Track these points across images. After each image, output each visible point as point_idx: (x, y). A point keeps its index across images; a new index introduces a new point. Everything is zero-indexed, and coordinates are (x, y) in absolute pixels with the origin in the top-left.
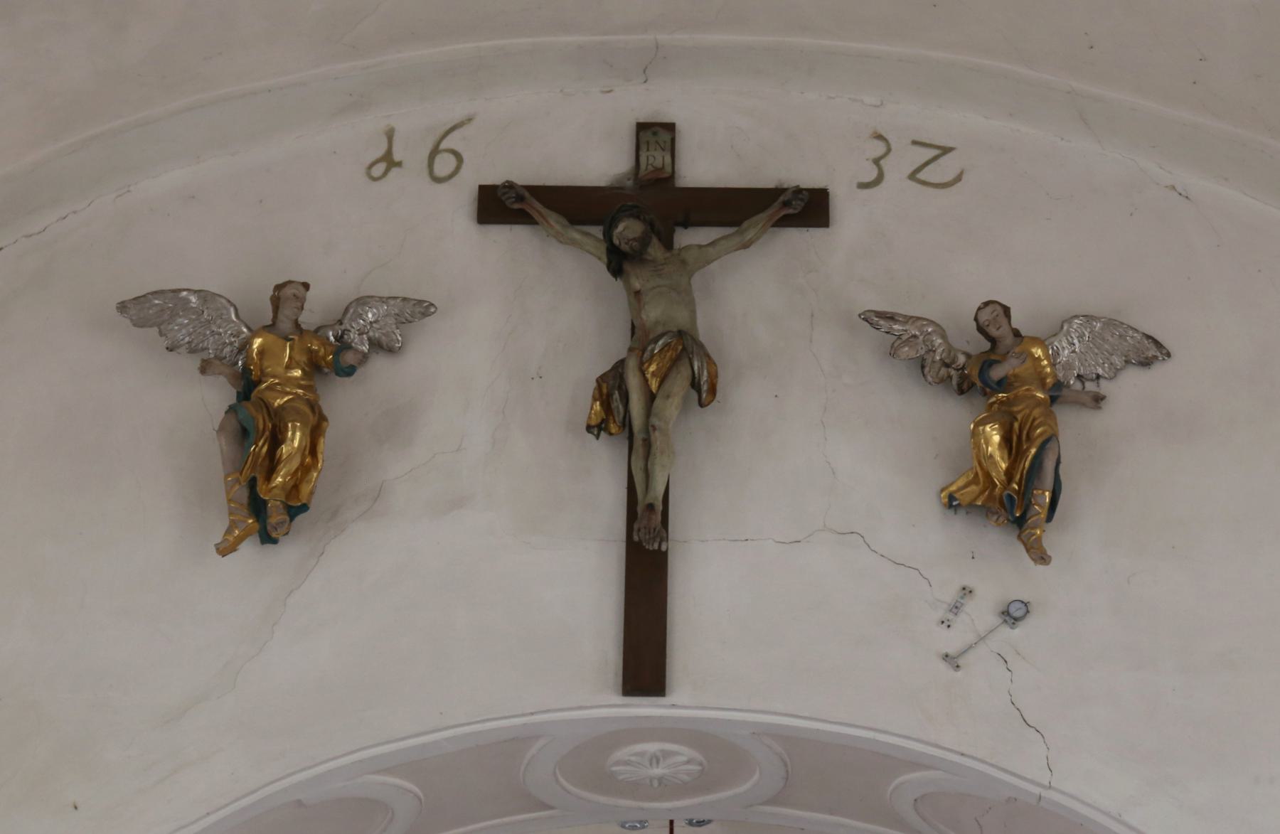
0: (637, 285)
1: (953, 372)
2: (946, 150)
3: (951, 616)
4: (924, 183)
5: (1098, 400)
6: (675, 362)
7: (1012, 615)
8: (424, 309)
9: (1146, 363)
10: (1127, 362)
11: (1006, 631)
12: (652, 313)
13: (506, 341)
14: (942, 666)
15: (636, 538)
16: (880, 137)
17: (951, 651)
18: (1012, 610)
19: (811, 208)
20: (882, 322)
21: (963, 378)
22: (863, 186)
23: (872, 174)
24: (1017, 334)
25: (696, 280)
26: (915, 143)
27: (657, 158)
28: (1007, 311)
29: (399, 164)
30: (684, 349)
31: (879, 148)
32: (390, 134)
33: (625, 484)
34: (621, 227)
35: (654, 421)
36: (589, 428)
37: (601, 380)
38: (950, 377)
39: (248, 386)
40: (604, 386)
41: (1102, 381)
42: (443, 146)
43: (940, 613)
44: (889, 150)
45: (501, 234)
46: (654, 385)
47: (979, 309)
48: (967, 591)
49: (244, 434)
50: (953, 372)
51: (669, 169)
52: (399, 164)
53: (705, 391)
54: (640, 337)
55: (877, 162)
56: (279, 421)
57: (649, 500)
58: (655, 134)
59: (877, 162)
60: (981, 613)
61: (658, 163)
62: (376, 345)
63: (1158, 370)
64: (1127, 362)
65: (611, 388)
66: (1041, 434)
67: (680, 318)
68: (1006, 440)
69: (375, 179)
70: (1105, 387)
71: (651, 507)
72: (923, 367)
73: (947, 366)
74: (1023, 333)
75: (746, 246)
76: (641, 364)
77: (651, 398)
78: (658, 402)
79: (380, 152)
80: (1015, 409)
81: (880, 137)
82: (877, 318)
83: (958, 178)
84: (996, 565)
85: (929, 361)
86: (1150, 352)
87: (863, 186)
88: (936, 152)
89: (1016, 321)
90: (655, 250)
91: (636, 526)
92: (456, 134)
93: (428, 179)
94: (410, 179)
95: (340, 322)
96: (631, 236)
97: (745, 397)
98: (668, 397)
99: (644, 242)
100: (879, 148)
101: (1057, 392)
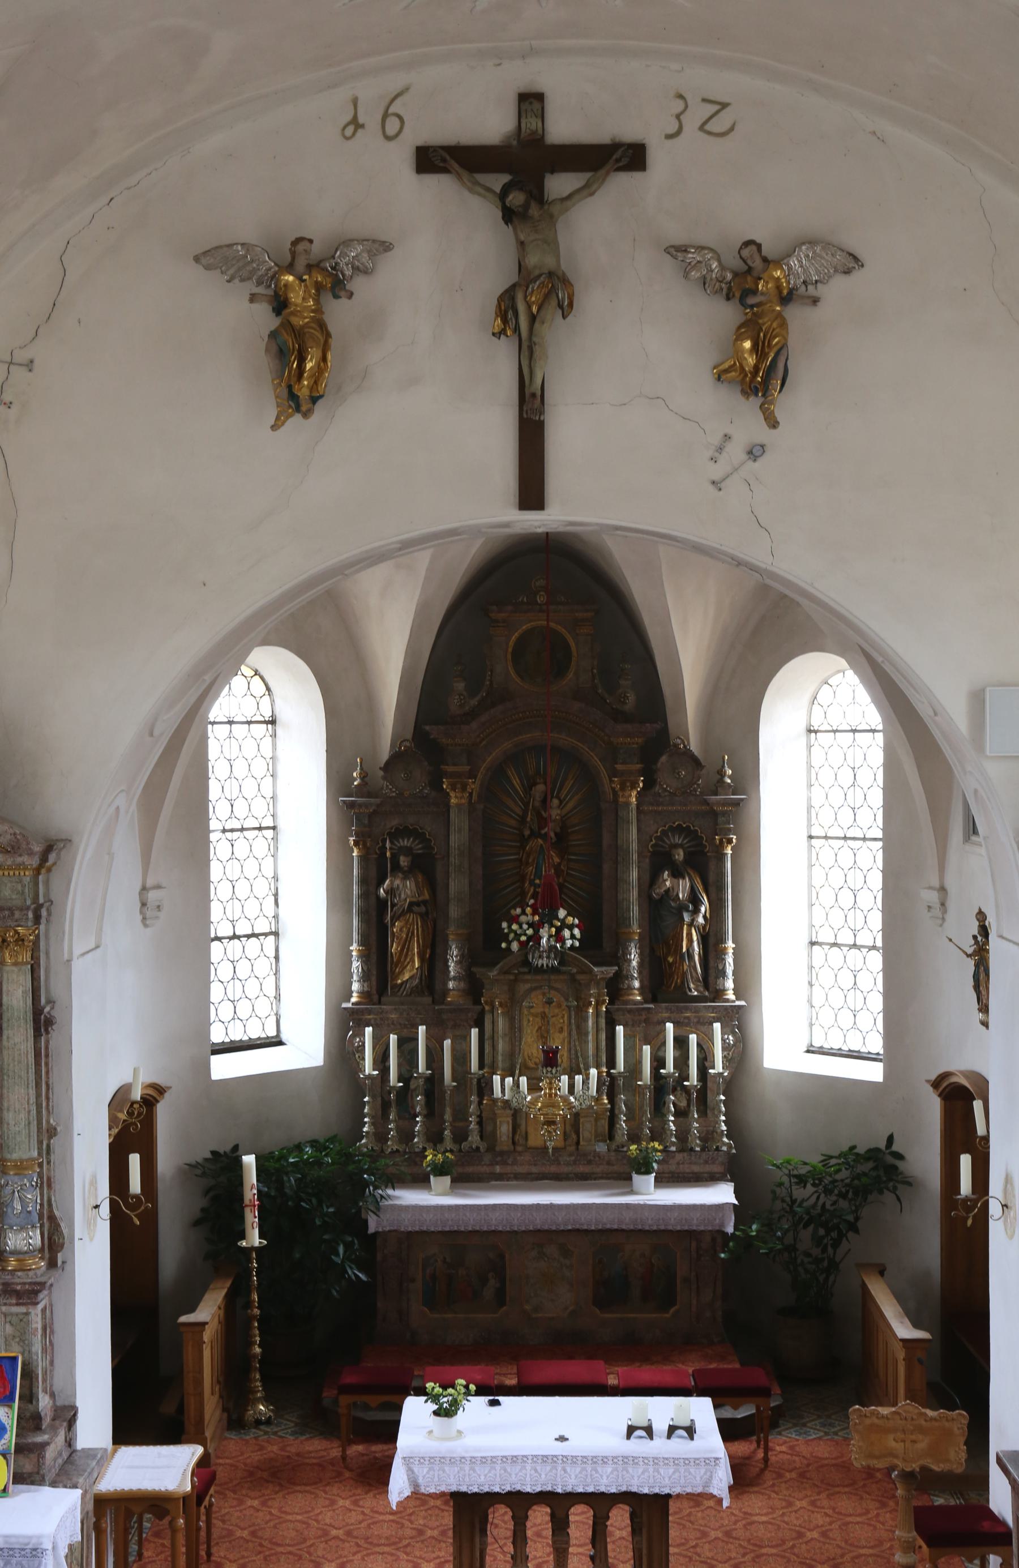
0: (522, 237)
1: (723, 285)
2: (724, 106)
3: (717, 454)
4: (709, 133)
5: (815, 301)
6: (547, 296)
7: (755, 452)
8: (387, 247)
9: (847, 272)
10: (836, 271)
11: (750, 463)
12: (532, 260)
13: (440, 256)
14: (711, 489)
15: (525, 416)
16: (681, 97)
17: (716, 478)
18: (754, 451)
19: (633, 157)
20: (679, 254)
21: (730, 289)
22: (669, 137)
23: (673, 128)
24: (765, 260)
25: (560, 226)
26: (704, 100)
27: (532, 123)
28: (759, 246)
29: (362, 126)
30: (553, 285)
31: (679, 105)
32: (355, 102)
33: (517, 366)
34: (510, 197)
35: (534, 339)
36: (494, 334)
37: (501, 298)
38: (722, 289)
39: (280, 304)
40: (503, 304)
41: (819, 285)
42: (390, 111)
43: (710, 453)
44: (686, 107)
45: (434, 182)
46: (534, 309)
47: (741, 248)
48: (727, 437)
49: (281, 354)
50: (723, 285)
51: (540, 131)
52: (362, 126)
53: (566, 309)
54: (525, 277)
55: (678, 117)
56: (300, 324)
57: (532, 390)
58: (531, 101)
59: (678, 117)
60: (736, 451)
61: (533, 127)
62: (356, 269)
63: (857, 275)
64: (836, 271)
65: (506, 307)
66: (777, 343)
67: (549, 262)
68: (755, 347)
69: (347, 138)
70: (822, 290)
71: (534, 395)
72: (704, 284)
73: (721, 282)
74: (770, 258)
75: (592, 194)
76: (526, 297)
77: (533, 319)
78: (537, 325)
79: (349, 117)
80: (760, 321)
81: (681, 97)
82: (677, 250)
83: (732, 129)
84: (745, 421)
85: (708, 279)
86: (853, 262)
87: (669, 137)
88: (717, 107)
89: (765, 251)
90: (534, 211)
91: (525, 409)
92: (398, 102)
93: (382, 137)
94: (370, 137)
95: (333, 257)
96: (517, 204)
97: (591, 301)
98: (543, 323)
99: (526, 206)
100: (679, 105)
101: (787, 298)
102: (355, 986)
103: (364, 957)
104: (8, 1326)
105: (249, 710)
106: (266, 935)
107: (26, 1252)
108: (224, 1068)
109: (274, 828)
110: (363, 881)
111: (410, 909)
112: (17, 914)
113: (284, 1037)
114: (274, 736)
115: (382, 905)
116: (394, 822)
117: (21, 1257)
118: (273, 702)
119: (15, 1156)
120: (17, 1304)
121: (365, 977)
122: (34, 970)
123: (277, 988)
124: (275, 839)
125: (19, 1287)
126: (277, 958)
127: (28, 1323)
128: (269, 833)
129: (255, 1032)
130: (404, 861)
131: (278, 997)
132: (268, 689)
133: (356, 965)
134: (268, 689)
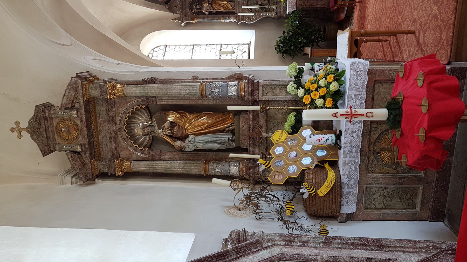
102: (232, 20)
103: (224, 18)
104: (268, 95)
105: (162, 52)
106: (221, 47)
107: (238, 87)
108: (252, 57)
109: (193, 45)
110: (204, 19)
111: (211, 4)
112: (104, 89)
113: (249, 43)
114: (170, 45)
115: (210, 13)
116: (188, 10)
117: (239, 89)
118: (161, 46)
119: (198, 91)
120: (259, 90)
121: (230, 18)
122: (128, 83)
123: (236, 44)
124: (196, 45)
125: (250, 89)
126: (228, 45)
127: (267, 85)
128: (195, 46)
129: (247, 50)
130: (198, 7)
131: (238, 44)
132: (157, 47)
133: (227, 20)
134: (157, 47)
